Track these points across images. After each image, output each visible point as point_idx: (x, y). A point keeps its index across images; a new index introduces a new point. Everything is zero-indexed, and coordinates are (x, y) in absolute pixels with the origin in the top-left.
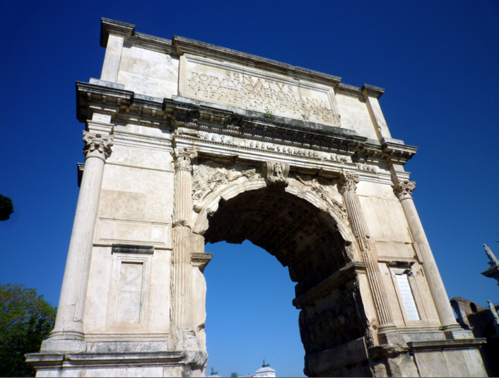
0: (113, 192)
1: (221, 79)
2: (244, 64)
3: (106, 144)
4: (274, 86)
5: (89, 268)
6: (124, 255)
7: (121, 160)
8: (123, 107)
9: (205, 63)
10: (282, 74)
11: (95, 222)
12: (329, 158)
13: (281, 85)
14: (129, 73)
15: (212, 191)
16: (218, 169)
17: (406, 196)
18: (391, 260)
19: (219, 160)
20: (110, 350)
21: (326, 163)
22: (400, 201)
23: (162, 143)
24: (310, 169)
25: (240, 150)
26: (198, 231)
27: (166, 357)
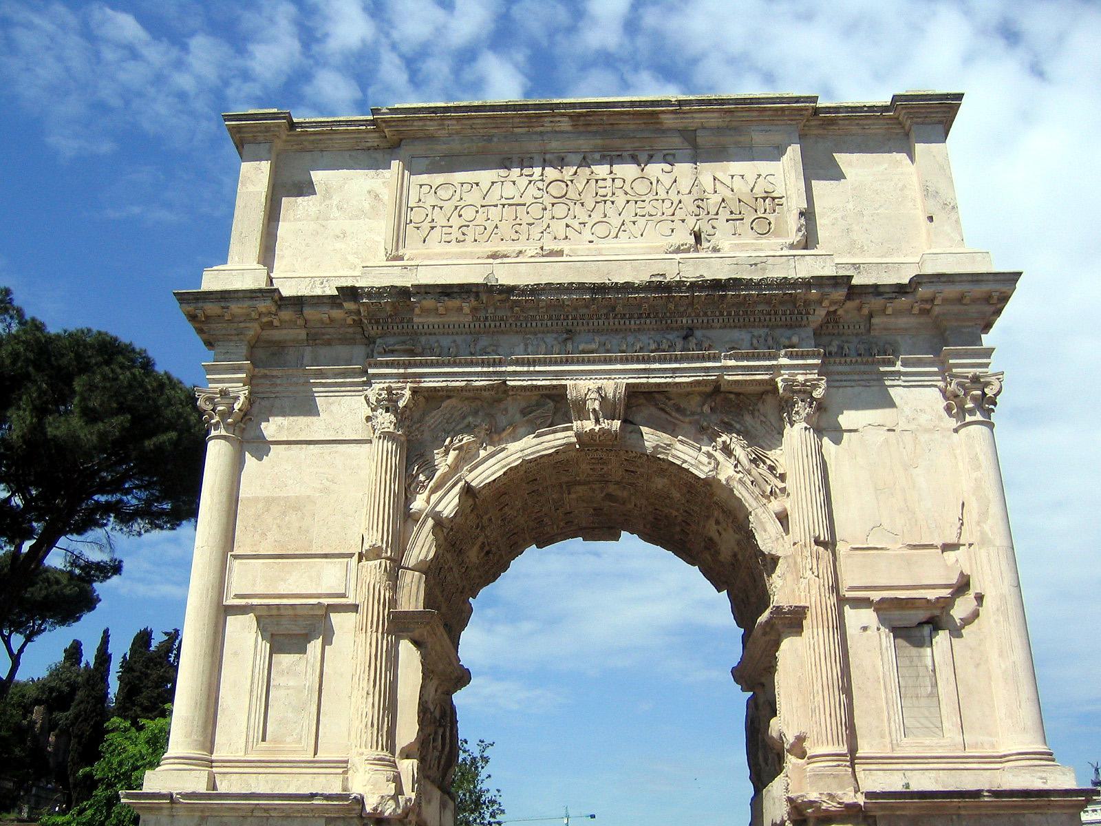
0: (256, 500)
1: (485, 186)
16: (470, 419)
18: (876, 596)
19: (471, 394)
27: (325, 802)
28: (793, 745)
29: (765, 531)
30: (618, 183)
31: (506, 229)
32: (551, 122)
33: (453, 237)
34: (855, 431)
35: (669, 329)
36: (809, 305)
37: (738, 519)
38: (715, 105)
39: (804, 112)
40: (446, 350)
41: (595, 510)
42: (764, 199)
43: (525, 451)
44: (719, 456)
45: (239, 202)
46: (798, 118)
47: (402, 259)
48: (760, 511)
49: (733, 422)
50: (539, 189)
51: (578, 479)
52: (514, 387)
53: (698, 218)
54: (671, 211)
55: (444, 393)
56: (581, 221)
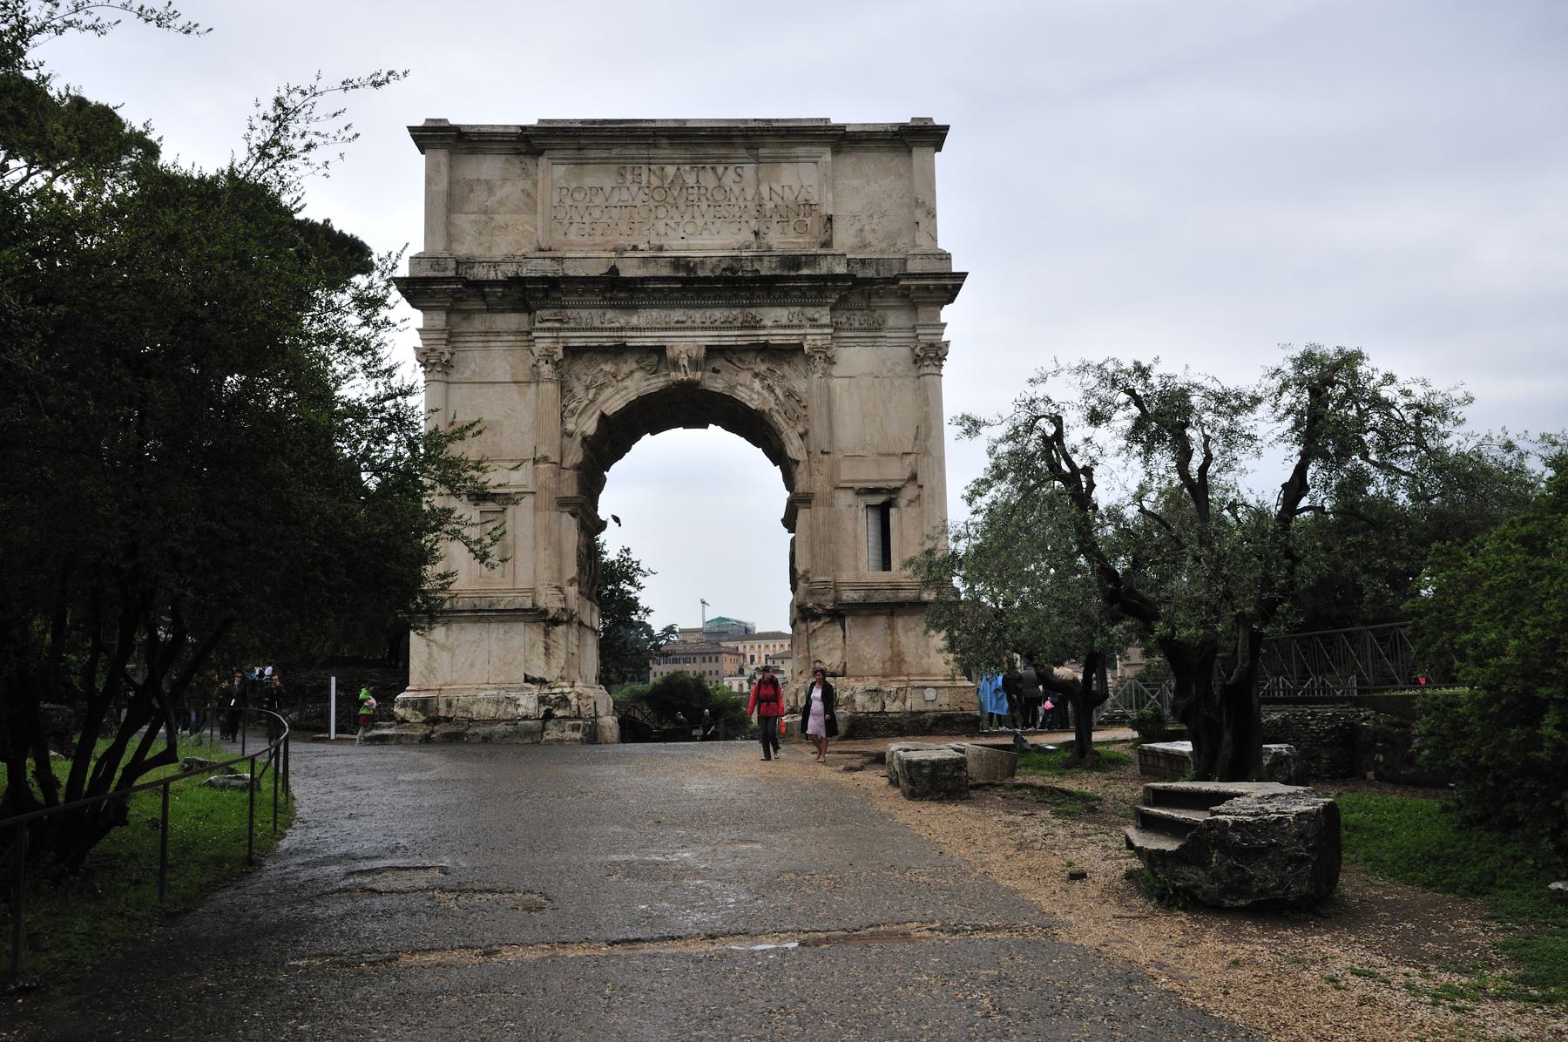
1: (607, 190)
4: (708, 179)
7: (468, 374)
8: (456, 296)
9: (581, 162)
10: (724, 145)
12: (784, 321)
13: (720, 169)
16: (603, 366)
17: (927, 370)
18: (857, 486)
20: (475, 606)
21: (774, 332)
23: (518, 338)
25: (629, 334)
28: (803, 576)
30: (703, 191)
31: (624, 228)
35: (735, 306)
40: (584, 320)
42: (804, 205)
44: (766, 393)
47: (550, 250)
48: (789, 432)
54: (739, 214)
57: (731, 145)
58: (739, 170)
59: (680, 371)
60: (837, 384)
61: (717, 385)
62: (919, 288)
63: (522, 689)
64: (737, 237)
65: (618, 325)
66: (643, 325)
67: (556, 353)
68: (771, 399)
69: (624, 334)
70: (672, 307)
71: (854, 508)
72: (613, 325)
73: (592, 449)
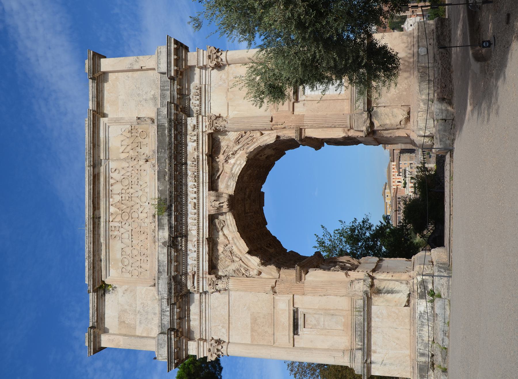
2: (99, 221)
3: (215, 345)
4: (116, 188)
5: (310, 349)
6: (299, 327)
7: (224, 330)
8: (180, 334)
9: (108, 260)
10: (99, 179)
11: (277, 347)
12: (195, 144)
13: (112, 181)
14: (137, 327)
15: (241, 259)
17: (224, 60)
19: (211, 252)
20: (360, 335)
21: (201, 150)
22: (229, 65)
23: (204, 300)
24: (209, 167)
25: (201, 236)
26: (277, 275)
28: (346, 133)
29: (267, 140)
30: (124, 191)
31: (143, 237)
32: (96, 219)
33: (145, 259)
34: (228, 103)
35: (186, 175)
36: (178, 119)
37: (261, 150)
38: (90, 151)
39: (95, 115)
41: (253, 202)
42: (132, 133)
43: (234, 231)
44: (237, 156)
45: (127, 347)
46: (97, 118)
49: (224, 150)
50: (125, 224)
51: (243, 210)
52: (209, 235)
53: (139, 160)
55: (210, 262)
56: (140, 208)
57: (99, 174)
58: (113, 170)
59: (222, 206)
60: (233, 114)
61: (233, 185)
62: (176, 65)
63: (414, 309)
64: (148, 172)
65: (196, 243)
66: (196, 227)
67: (212, 278)
68: (241, 152)
69: (201, 239)
70: (187, 210)
71: (305, 102)
72: (196, 245)
73: (270, 260)
